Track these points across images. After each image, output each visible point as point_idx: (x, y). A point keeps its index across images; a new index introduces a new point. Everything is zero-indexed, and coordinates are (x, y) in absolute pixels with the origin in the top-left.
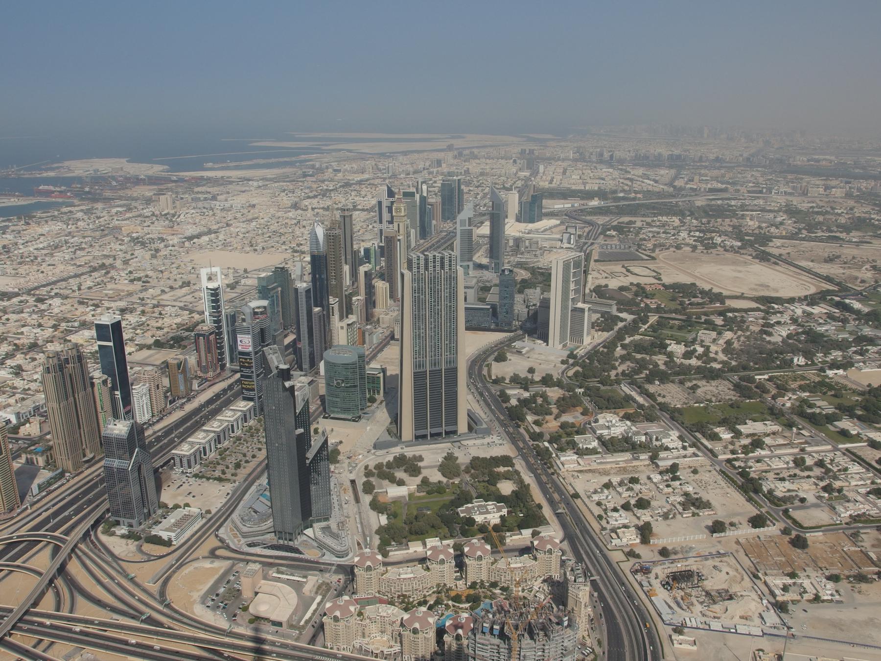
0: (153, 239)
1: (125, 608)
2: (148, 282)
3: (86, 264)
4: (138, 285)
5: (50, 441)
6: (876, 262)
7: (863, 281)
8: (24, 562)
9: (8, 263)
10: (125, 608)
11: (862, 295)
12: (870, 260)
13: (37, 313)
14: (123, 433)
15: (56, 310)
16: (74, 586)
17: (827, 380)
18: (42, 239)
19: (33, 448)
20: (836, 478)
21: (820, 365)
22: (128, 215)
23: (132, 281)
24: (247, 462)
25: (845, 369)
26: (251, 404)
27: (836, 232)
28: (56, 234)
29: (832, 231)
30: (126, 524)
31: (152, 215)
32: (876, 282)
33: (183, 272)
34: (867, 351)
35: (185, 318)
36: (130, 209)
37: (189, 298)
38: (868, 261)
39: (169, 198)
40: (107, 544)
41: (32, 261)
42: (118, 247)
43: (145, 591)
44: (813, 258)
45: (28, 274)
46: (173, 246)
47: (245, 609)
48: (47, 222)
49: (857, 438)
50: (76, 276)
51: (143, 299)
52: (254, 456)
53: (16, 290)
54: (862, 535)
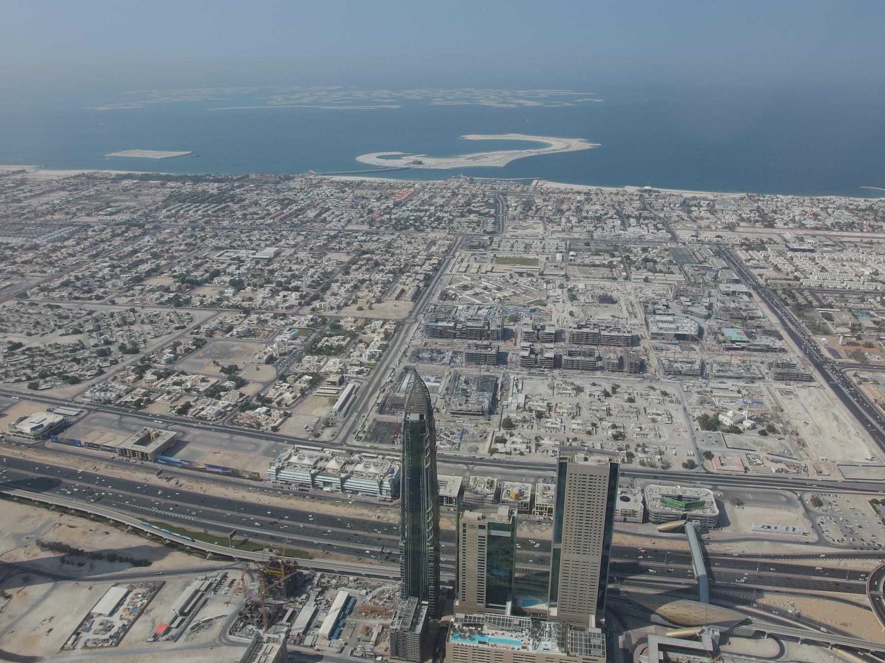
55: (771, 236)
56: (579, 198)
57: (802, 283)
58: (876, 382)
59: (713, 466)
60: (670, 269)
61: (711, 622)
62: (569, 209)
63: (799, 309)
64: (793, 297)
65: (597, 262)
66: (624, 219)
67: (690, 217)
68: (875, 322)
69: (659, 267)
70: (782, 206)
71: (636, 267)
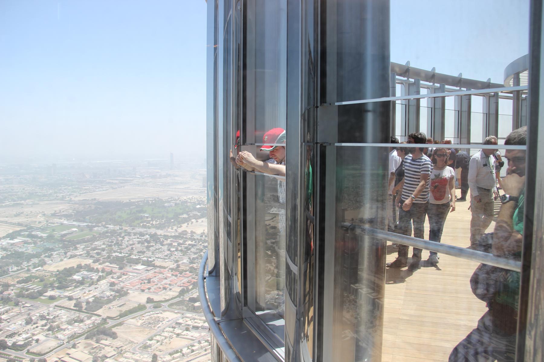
6: (44, 212)
7: (40, 222)
11: (41, 229)
12: (41, 212)
17: (33, 275)
20: (53, 322)
21: (26, 268)
25: (42, 266)
27: (17, 201)
29: (15, 201)
32: (47, 221)
34: (52, 255)
38: (40, 213)
44: (7, 216)
49: (60, 297)
54: (77, 345)
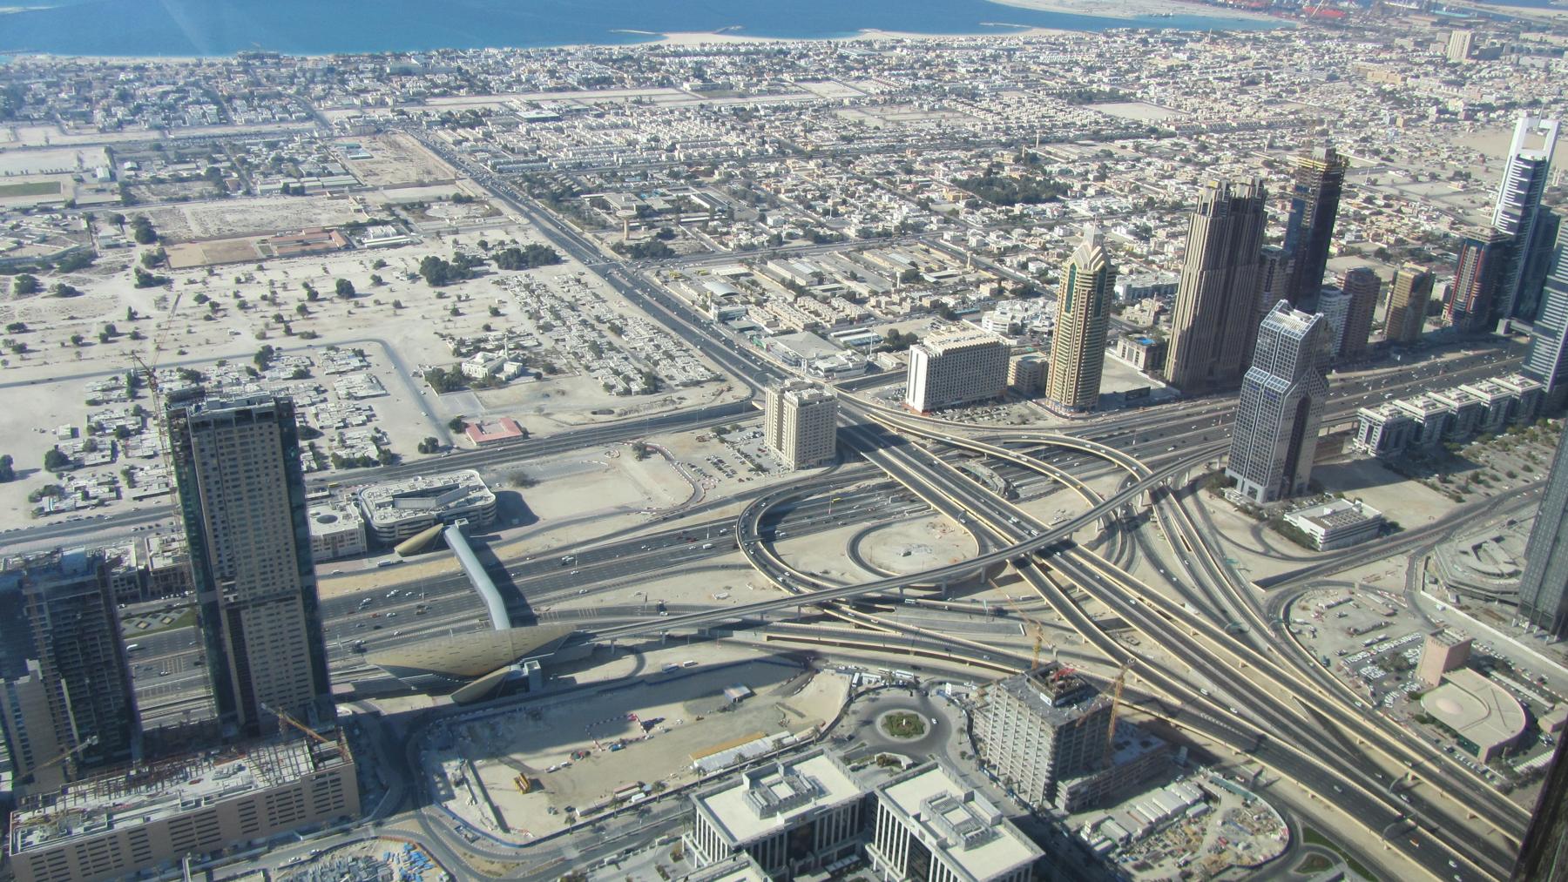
0: (1419, 99)
1: (1208, 603)
2: (1392, 161)
3: (1291, 113)
4: (1375, 161)
5: (1165, 334)
8: (1082, 480)
9: (1170, 90)
10: (1208, 603)
13: (1197, 164)
14: (1297, 331)
15: (1226, 167)
16: (1141, 542)
18: (1230, 67)
19: (1137, 336)
22: (1382, 56)
23: (1361, 152)
24: (1496, 479)
26: (1535, 384)
28: (1256, 64)
30: (1246, 489)
31: (1427, 62)
33: (1462, 157)
35: (1443, 226)
36: (1388, 48)
37: (1460, 200)
39: (1469, 38)
40: (1207, 507)
41: (1207, 94)
42: (1353, 98)
43: (1246, 591)
45: (1195, 111)
46: (1456, 114)
47: (1415, 696)
48: (1244, 46)
50: (1270, 126)
51: (1374, 183)
52: (1512, 475)
53: (1172, 128)
55: (488, 107)
56: (122, 76)
57: (551, 164)
58: (687, 279)
59: (467, 441)
60: (325, 168)
61: (523, 652)
62: (106, 96)
63: (556, 200)
64: (543, 185)
65: (185, 174)
66: (224, 105)
67: (346, 91)
68: (667, 201)
69: (304, 168)
70: (497, 63)
71: (262, 173)
